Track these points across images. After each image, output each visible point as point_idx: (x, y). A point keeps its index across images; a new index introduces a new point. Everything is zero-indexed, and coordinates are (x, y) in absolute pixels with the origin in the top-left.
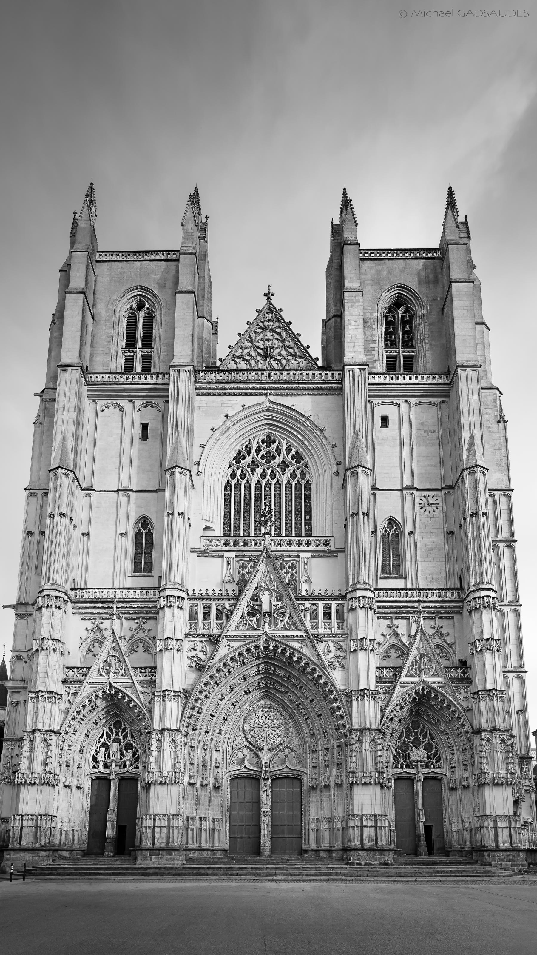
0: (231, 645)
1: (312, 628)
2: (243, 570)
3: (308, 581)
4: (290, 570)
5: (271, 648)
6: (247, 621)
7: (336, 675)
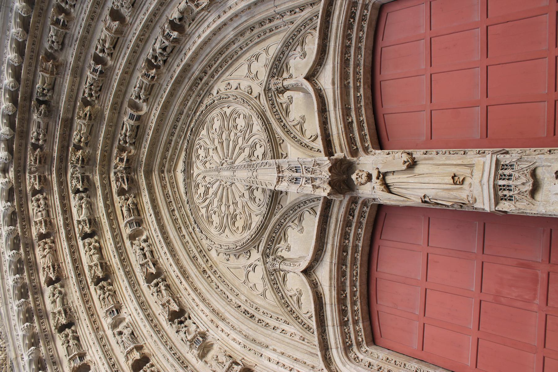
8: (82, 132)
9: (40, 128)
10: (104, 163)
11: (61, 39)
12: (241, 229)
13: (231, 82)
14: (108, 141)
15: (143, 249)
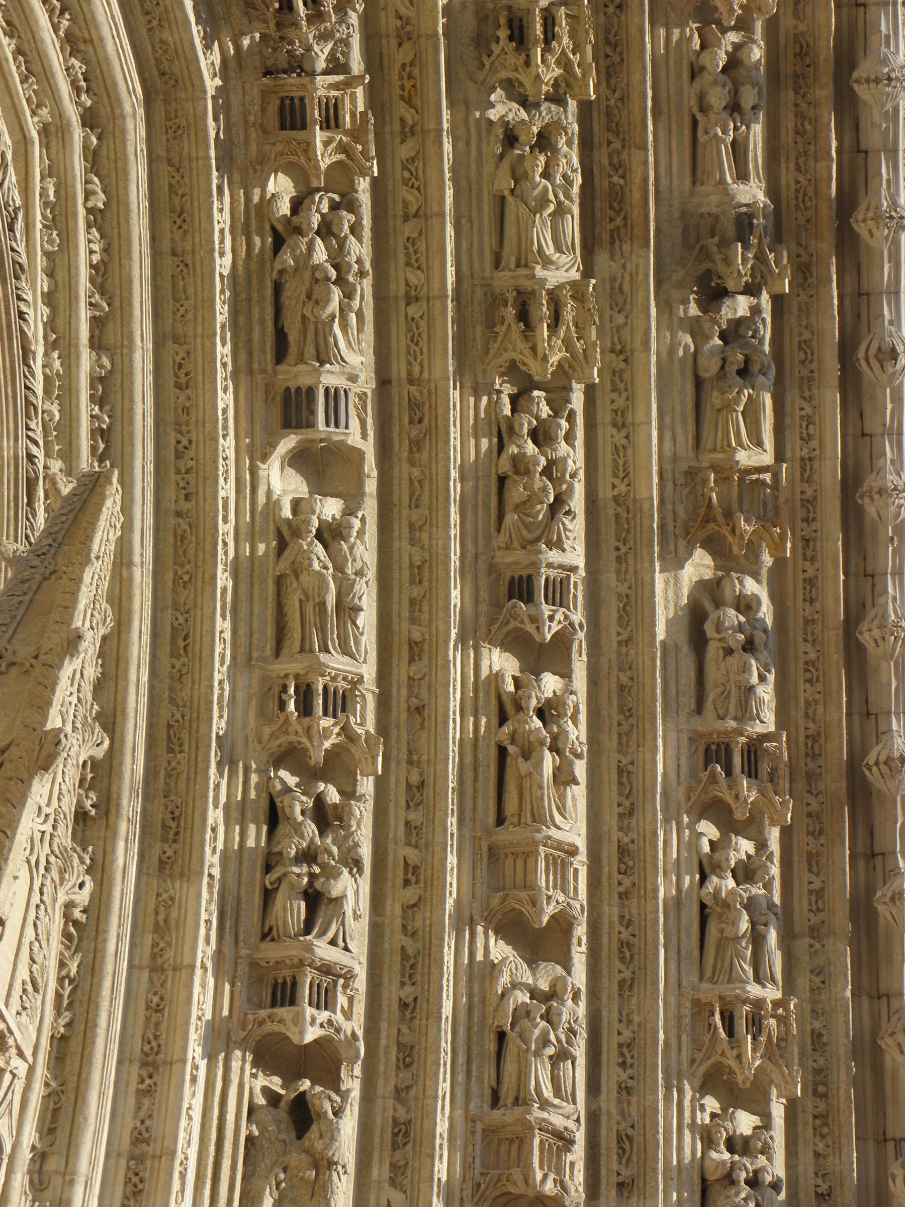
8: (552, 208)
9: (734, 143)
10: (404, 55)
11: (713, 674)
14: (405, 194)
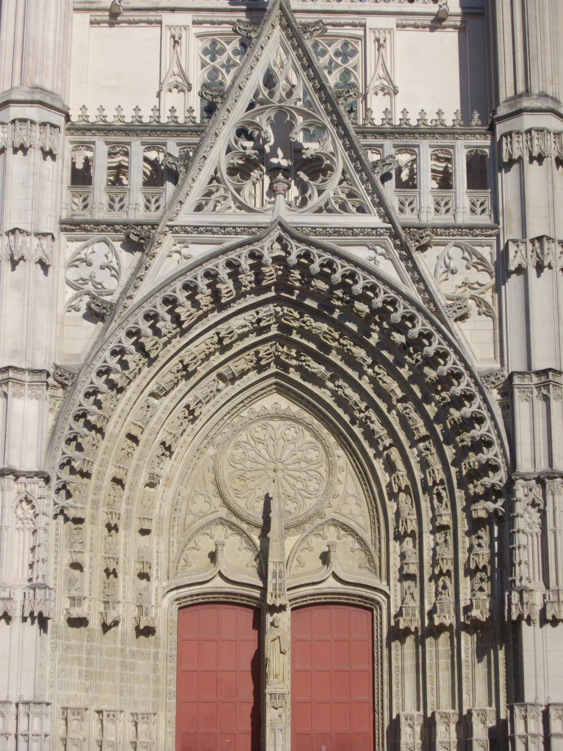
0: (185, 251)
1: (401, 211)
2: (213, 59)
3: (391, 90)
4: (339, 60)
5: (293, 259)
6: (226, 190)
7: (467, 333)
12: (234, 486)
13: (344, 474)
15: (211, 392)
